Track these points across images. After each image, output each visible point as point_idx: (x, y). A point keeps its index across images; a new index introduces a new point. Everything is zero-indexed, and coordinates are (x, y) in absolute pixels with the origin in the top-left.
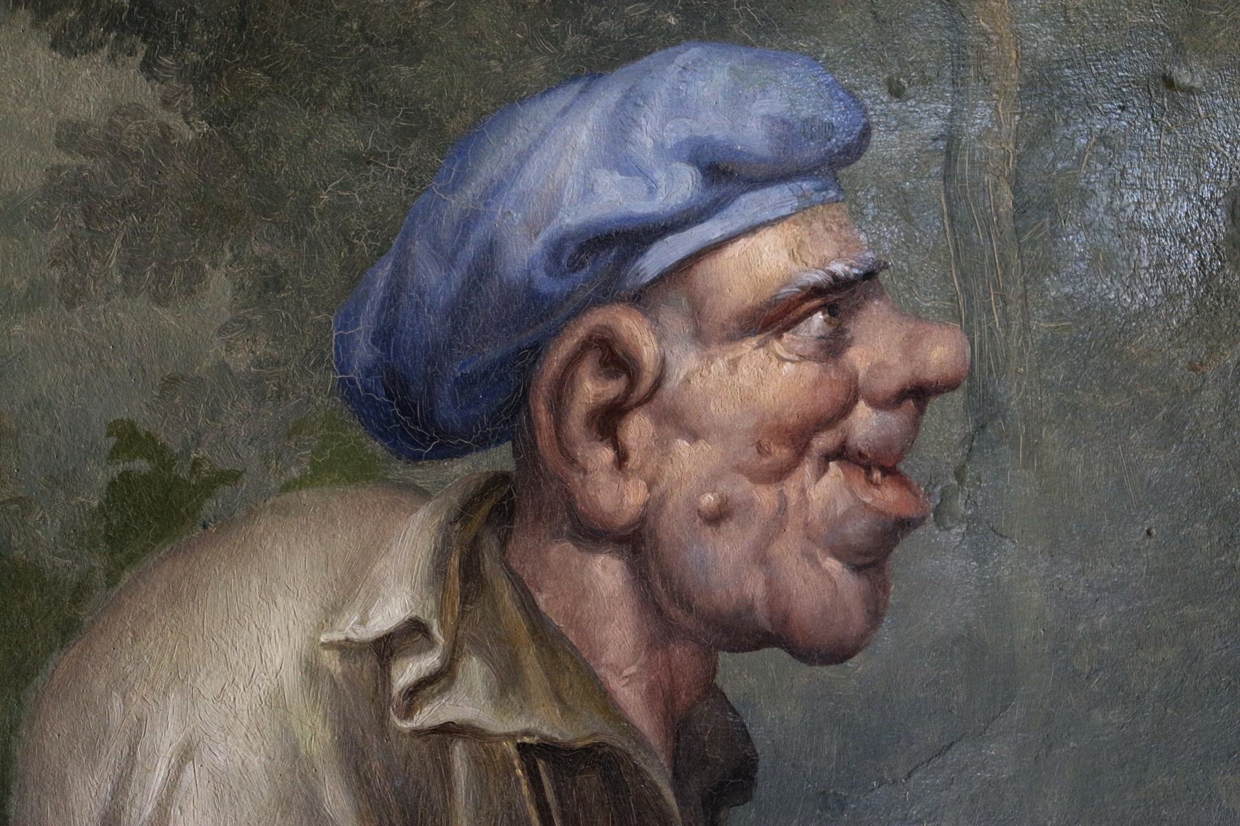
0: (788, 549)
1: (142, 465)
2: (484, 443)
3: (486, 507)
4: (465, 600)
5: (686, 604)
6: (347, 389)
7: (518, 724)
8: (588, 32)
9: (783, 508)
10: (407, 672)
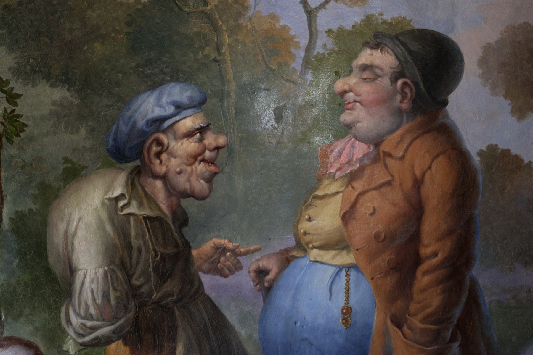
0: (193, 179)
1: (69, 165)
2: (135, 160)
3: (135, 172)
4: (132, 189)
5: (174, 190)
6: (108, 150)
7: (142, 213)
8: (152, 81)
9: (192, 171)
10: (121, 203)
